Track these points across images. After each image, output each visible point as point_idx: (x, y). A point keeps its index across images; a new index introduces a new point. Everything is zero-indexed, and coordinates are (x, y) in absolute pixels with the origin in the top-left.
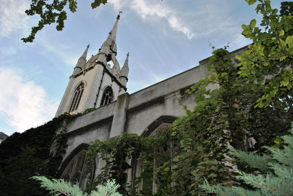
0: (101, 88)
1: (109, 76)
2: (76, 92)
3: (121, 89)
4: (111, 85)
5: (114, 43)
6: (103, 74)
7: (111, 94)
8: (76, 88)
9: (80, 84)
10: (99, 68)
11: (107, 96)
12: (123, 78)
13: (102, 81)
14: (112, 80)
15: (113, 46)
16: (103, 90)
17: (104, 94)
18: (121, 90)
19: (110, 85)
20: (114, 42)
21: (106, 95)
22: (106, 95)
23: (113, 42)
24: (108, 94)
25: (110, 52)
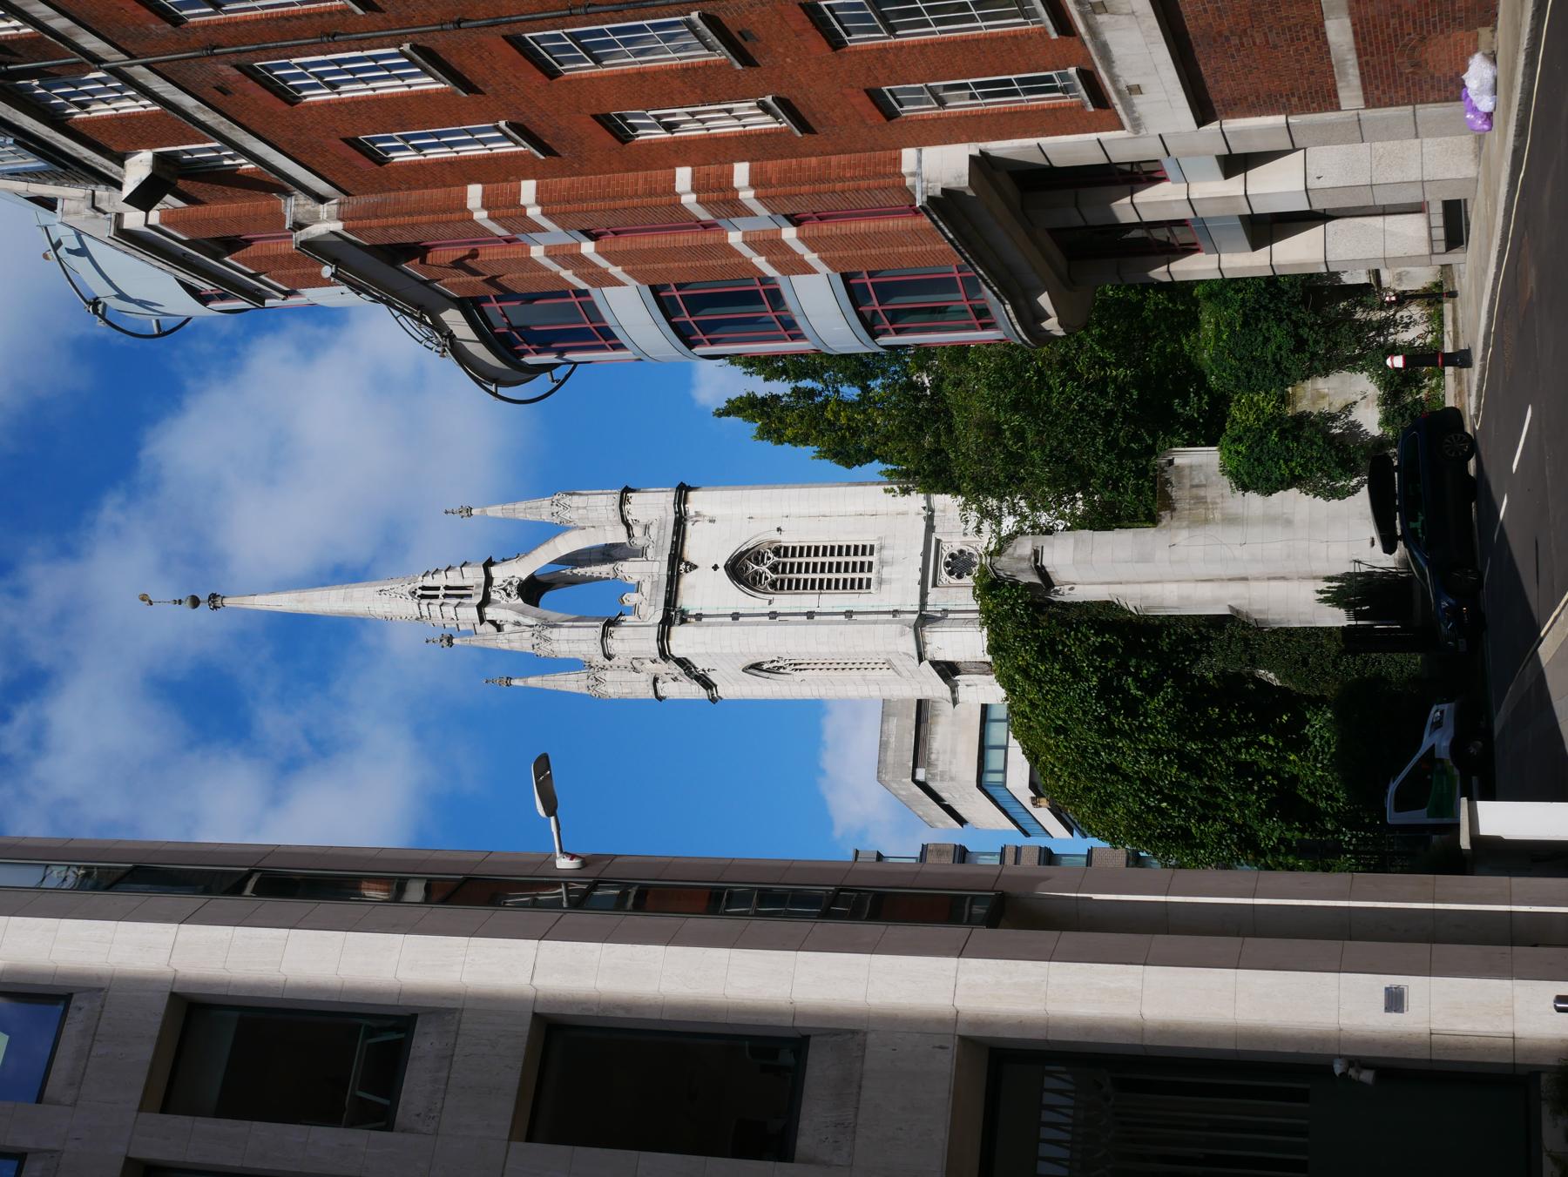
1: (682, 586)
3: (691, 512)
4: (715, 568)
5: (423, 588)
6: (699, 617)
7: (756, 555)
8: (772, 675)
9: (756, 672)
10: (683, 641)
11: (774, 569)
13: (735, 616)
15: (447, 588)
16: (771, 597)
18: (698, 514)
19: (722, 570)
20: (419, 592)
21: (774, 576)
22: (774, 576)
23: (423, 597)
24: (764, 568)
25: (509, 595)
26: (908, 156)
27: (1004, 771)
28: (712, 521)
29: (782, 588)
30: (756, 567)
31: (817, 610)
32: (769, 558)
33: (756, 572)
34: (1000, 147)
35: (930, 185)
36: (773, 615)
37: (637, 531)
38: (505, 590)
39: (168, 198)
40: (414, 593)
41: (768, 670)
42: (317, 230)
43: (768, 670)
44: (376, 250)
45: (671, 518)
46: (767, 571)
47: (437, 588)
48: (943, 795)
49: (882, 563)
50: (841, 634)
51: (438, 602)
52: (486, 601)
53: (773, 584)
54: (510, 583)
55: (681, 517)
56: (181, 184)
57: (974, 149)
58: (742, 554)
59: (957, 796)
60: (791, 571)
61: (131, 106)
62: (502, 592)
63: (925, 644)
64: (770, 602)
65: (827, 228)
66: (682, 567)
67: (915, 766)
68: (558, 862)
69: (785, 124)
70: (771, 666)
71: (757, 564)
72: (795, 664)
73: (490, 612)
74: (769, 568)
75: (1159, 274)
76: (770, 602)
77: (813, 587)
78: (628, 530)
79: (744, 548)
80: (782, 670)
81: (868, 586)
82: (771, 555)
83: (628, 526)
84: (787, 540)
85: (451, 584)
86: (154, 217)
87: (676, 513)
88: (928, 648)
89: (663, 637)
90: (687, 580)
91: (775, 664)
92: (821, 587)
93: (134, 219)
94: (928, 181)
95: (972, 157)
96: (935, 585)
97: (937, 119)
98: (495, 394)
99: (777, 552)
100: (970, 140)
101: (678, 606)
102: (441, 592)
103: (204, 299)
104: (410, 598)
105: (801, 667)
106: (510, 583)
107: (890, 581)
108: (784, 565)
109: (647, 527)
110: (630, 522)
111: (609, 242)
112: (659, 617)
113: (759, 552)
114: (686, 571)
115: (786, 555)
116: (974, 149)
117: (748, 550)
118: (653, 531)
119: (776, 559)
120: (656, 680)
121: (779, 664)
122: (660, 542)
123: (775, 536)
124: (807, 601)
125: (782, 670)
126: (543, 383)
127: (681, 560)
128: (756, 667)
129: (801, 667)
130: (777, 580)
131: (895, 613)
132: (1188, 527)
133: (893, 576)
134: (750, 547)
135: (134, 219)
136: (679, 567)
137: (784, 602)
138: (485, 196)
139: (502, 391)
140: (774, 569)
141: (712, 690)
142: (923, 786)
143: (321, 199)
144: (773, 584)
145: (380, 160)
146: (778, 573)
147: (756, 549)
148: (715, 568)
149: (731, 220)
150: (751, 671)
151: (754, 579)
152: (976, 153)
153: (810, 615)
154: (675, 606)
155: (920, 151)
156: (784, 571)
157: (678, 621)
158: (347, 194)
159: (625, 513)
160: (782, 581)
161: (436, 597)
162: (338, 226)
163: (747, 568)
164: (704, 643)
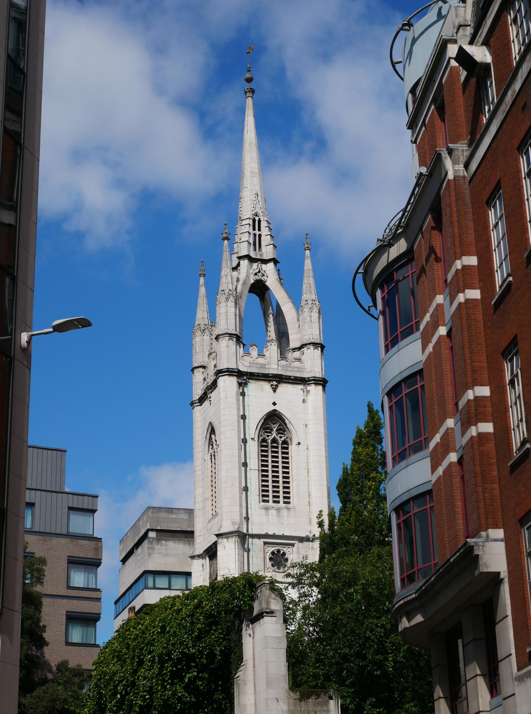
0: (247, 437)
1: (262, 383)
2: (210, 454)
3: (309, 388)
4: (274, 404)
5: (259, 221)
6: (243, 394)
7: (283, 429)
9: (210, 431)
11: (274, 441)
12: (305, 349)
13: (244, 417)
14: (272, 388)
15: (260, 236)
16: (256, 439)
17: (263, 443)
18: (308, 392)
19: (273, 408)
20: (257, 218)
21: (269, 441)
22: (269, 441)
23: (254, 221)
24: (274, 435)
25: (256, 274)
26: (499, 533)
27: (155, 588)
28: (304, 401)
29: (262, 446)
30: (275, 429)
31: (248, 469)
32: (281, 437)
33: (272, 430)
34: (505, 590)
35: (481, 547)
36: (245, 441)
37: (297, 354)
38: (259, 272)
39: (465, 73)
40: (257, 215)
41: (210, 438)
42: (448, 163)
43: (210, 438)
44: (438, 199)
45: (306, 375)
46: (273, 436)
47: (259, 230)
48: (140, 549)
49: (279, 510)
50: (233, 484)
51: (251, 231)
52: (252, 260)
53: (264, 440)
54: (263, 275)
55: (306, 381)
56: (473, 80)
57: (504, 574)
58: (283, 421)
59: (139, 558)
60: (273, 452)
61: (516, 49)
62: (258, 270)
63: (228, 538)
64: (253, 439)
65: (457, 480)
66: (275, 383)
67: (157, 531)
68: (25, 333)
69: (516, 455)
70: (213, 440)
71: (277, 430)
72: (214, 455)
73: (245, 263)
74: (274, 438)
75: (438, 692)
76: (253, 439)
77: (263, 466)
78: (297, 348)
79: (287, 422)
80: (211, 447)
81: (264, 501)
82: (283, 439)
83: (300, 348)
84: (293, 449)
85: (263, 238)
86: (454, 63)
87: (309, 378)
88: (225, 540)
89: (230, 372)
90: (266, 386)
91: (215, 443)
92: (263, 471)
93: (452, 50)
94: (483, 546)
95: (499, 573)
96: (265, 543)
97: (520, 552)
98: (357, 272)
99: (285, 442)
100: (509, 572)
101: (250, 381)
102: (257, 233)
103: (413, 91)
104: (253, 213)
105: (213, 459)
106: (263, 275)
107: (267, 514)
108: (277, 447)
109: (299, 360)
110: (303, 350)
111: (446, 343)
112: (243, 369)
113: (285, 431)
114: (272, 385)
115: (283, 448)
116: (504, 574)
117: (286, 424)
118: (297, 364)
119: (280, 442)
120: (204, 367)
121: (214, 445)
122: (290, 369)
123: (295, 441)
124: (254, 462)
125: (211, 447)
126: (367, 301)
127: (279, 382)
128: (212, 431)
129: (213, 459)
130: (267, 443)
131: (247, 519)
132: (289, 710)
133: (270, 517)
134: (288, 425)
135: (452, 50)
136: (274, 381)
137: (253, 447)
138: (470, 267)
139: (360, 277)
140: (274, 441)
141: (198, 403)
142: (145, 536)
143: (467, 166)
144: (264, 440)
145: (489, 203)
146: (271, 443)
147: (287, 429)
148: (274, 404)
149: (460, 422)
150: (210, 427)
151: (268, 428)
152: (502, 576)
153: (245, 465)
154: (250, 379)
155: (502, 540)
156: (272, 447)
157: (240, 381)
158: (470, 182)
159: (308, 346)
160: (266, 446)
161: (254, 229)
162: (450, 176)
163: (274, 424)
164: (226, 398)
